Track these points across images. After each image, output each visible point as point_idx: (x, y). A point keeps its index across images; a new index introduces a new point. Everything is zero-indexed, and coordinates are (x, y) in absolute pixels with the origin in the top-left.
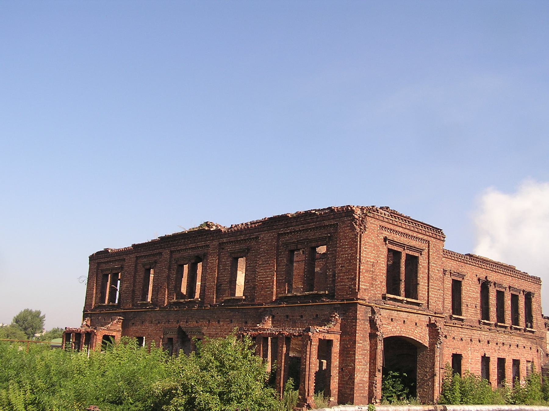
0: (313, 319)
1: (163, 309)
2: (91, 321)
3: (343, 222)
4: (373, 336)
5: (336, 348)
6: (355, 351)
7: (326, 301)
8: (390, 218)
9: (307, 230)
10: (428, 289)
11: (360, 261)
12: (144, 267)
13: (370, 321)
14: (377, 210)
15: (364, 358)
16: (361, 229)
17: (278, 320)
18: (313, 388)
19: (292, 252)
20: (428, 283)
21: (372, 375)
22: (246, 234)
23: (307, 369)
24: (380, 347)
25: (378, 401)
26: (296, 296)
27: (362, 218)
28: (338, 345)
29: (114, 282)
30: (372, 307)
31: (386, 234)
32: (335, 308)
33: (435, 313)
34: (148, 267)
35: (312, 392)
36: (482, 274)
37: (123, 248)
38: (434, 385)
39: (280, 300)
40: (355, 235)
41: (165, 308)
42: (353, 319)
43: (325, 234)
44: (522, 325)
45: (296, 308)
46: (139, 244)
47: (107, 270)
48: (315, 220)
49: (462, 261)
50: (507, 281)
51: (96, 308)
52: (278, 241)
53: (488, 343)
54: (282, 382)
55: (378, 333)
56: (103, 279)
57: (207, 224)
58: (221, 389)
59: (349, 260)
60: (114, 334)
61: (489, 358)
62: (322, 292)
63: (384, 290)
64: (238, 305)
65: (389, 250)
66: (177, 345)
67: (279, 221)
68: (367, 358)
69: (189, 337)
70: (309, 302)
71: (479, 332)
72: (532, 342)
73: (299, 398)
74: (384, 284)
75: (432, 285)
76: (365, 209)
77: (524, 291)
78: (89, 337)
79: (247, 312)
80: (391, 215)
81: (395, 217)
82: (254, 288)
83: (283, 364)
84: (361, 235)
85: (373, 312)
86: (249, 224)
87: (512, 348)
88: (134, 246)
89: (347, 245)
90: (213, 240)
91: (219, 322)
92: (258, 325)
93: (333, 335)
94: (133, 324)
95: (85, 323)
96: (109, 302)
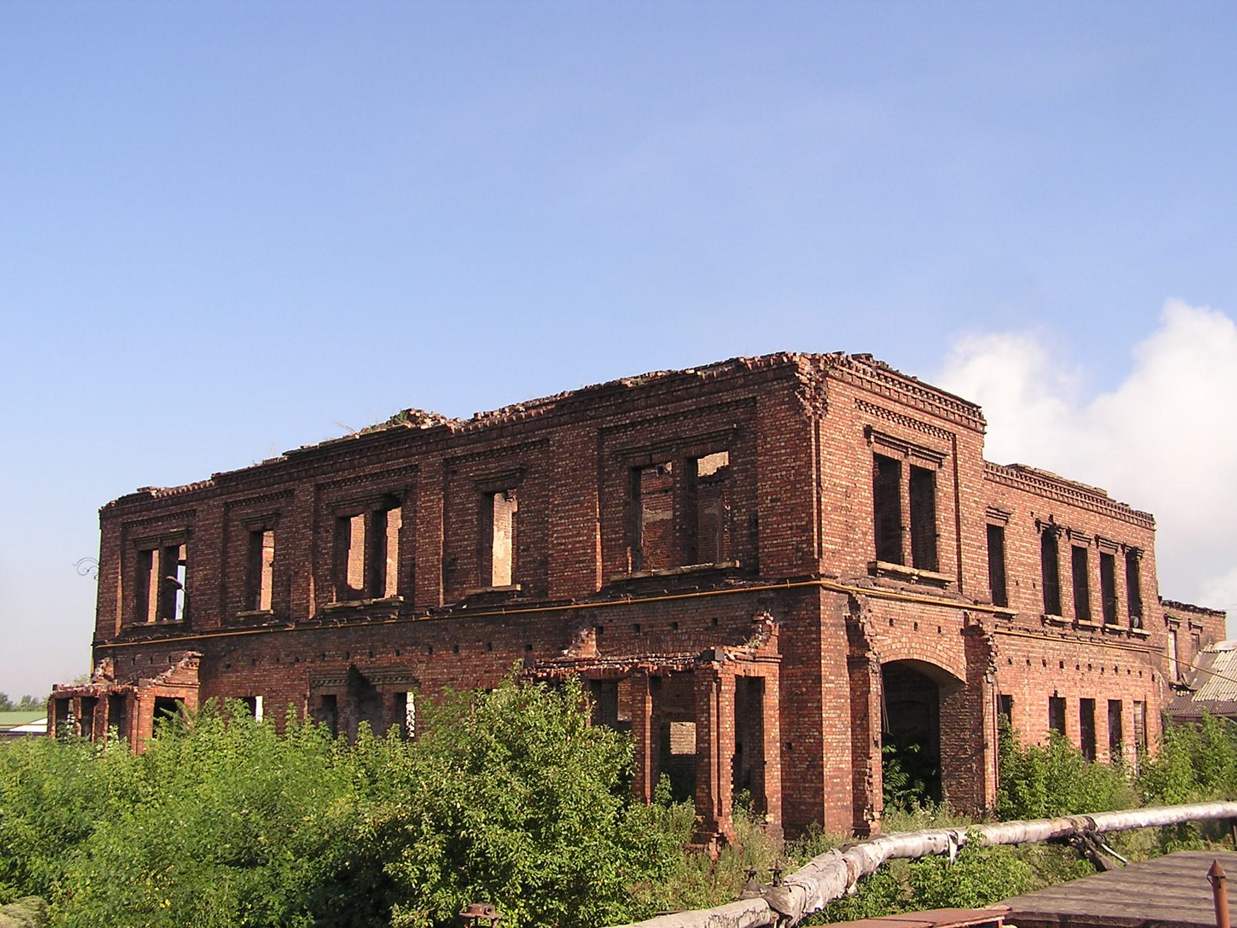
0: (706, 629)
1: (305, 626)
2: (115, 664)
3: (770, 393)
4: (857, 663)
5: (772, 697)
6: (820, 701)
7: (739, 585)
8: (875, 380)
10: (959, 547)
11: (819, 485)
12: (246, 527)
13: (848, 627)
14: (849, 363)
15: (839, 716)
16: (815, 407)
17: (613, 639)
18: (729, 794)
19: (637, 471)
20: (958, 534)
21: (860, 754)
22: (514, 435)
23: (714, 751)
24: (876, 686)
25: (877, 815)
26: (657, 578)
27: (817, 382)
28: (776, 689)
29: (169, 568)
30: (850, 595)
31: (868, 418)
32: (761, 601)
33: (976, 603)
34: (257, 527)
36: (1043, 509)
37: (188, 483)
38: (983, 770)
39: (614, 588)
40: (804, 422)
41: (310, 623)
44: (1123, 625)
45: (660, 605)
46: (232, 473)
47: (149, 539)
48: (696, 391)
49: (1003, 481)
51: (125, 633)
52: (600, 447)
53: (1062, 667)
54: (648, 785)
55: (870, 655)
56: (138, 562)
57: (408, 414)
58: (528, 813)
59: (793, 484)
60: (182, 693)
62: (724, 565)
63: (871, 549)
64: (507, 608)
65: (876, 456)
66: (348, 711)
67: (601, 398)
68: (847, 716)
69: (379, 689)
70: (694, 591)
71: (1043, 642)
72: (1142, 659)
73: (697, 822)
74: (871, 537)
75: (966, 538)
77: (1124, 546)
78: (120, 706)
79: (530, 624)
80: (878, 375)
81: (886, 378)
82: (544, 563)
83: (648, 742)
84: (817, 423)
85: (854, 606)
86: (521, 408)
87: (1106, 675)
88: (218, 477)
89: (783, 448)
90: (427, 452)
91: (456, 649)
92: (566, 652)
93: (764, 666)
94: (229, 666)
95: (100, 672)
96: (159, 618)
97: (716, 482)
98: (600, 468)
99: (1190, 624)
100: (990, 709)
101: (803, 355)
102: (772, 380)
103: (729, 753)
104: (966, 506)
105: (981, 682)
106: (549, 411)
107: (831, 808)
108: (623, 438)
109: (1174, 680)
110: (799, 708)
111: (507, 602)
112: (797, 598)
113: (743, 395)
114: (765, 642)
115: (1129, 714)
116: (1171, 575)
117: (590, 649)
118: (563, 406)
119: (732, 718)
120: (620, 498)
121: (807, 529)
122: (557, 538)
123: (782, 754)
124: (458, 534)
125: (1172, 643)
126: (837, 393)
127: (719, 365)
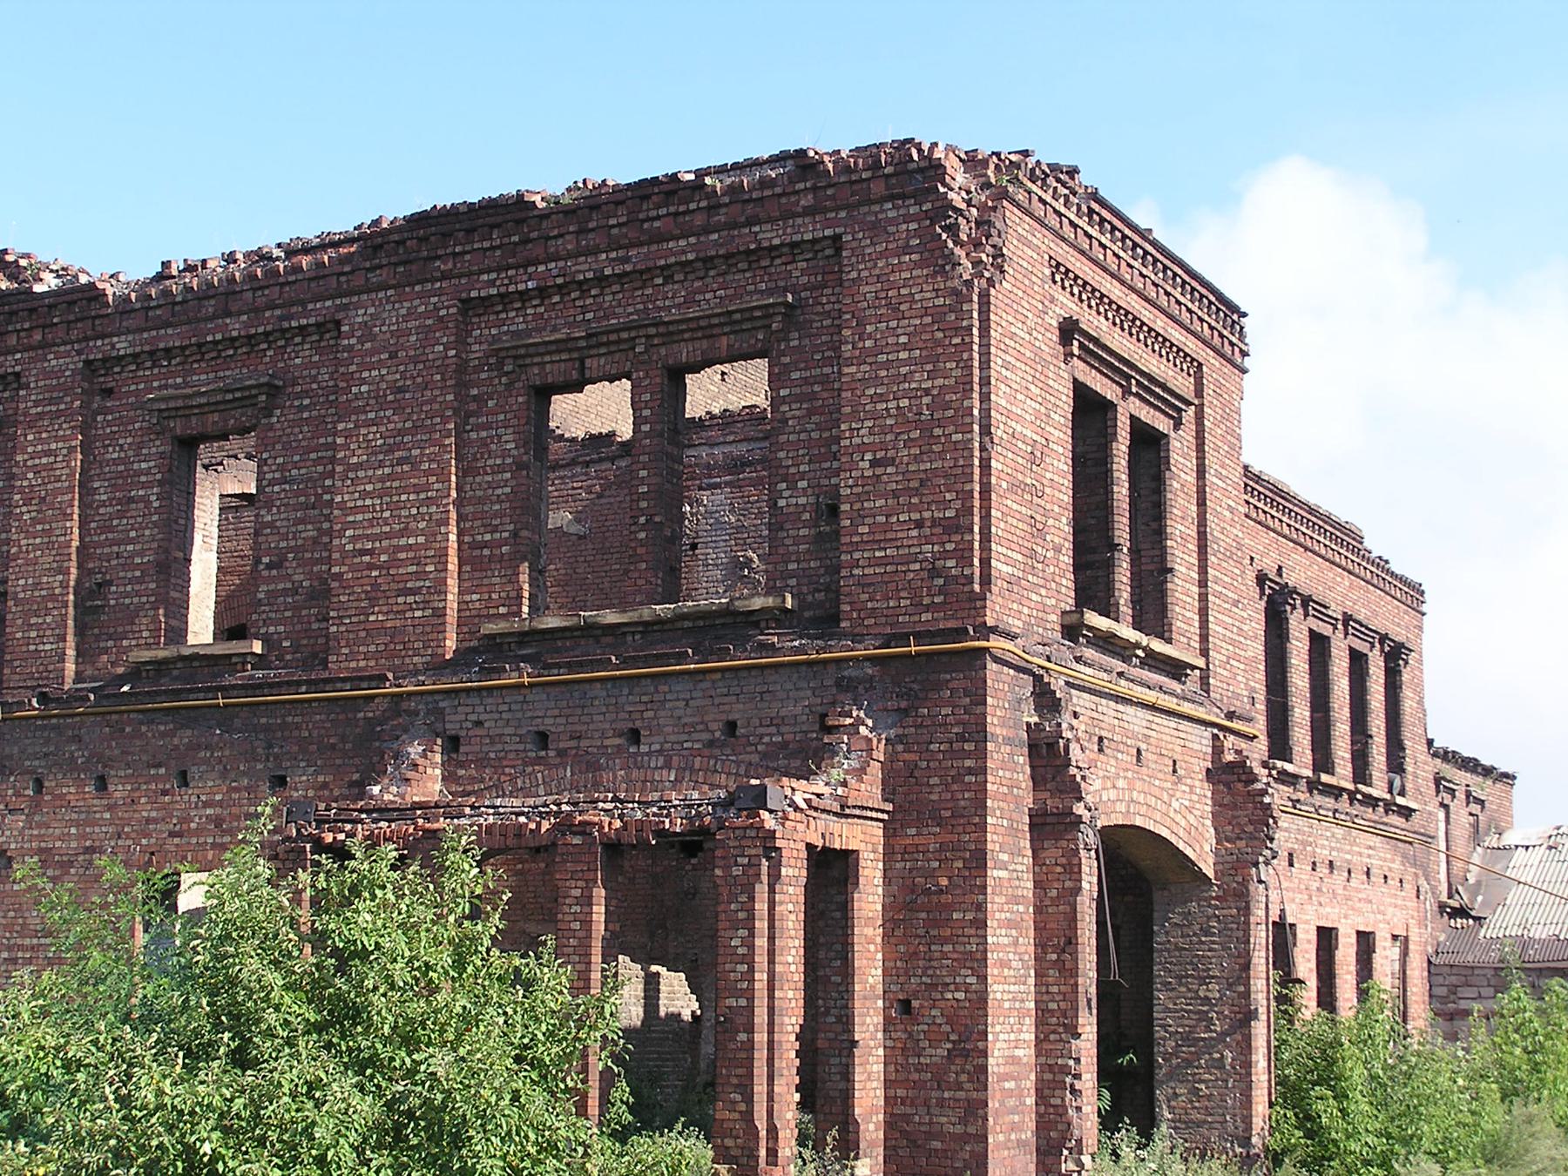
0: (711, 744)
3: (876, 229)
4: (1052, 825)
6: (981, 907)
7: (790, 647)
9: (643, 276)
10: (1203, 598)
11: (986, 430)
15: (1016, 943)
16: (977, 263)
21: (1053, 1026)
22: (256, 310)
26: (591, 631)
27: (982, 208)
28: (879, 881)
30: (1038, 679)
31: (1067, 305)
32: (847, 685)
33: (1231, 716)
35: (788, 1147)
36: (1270, 552)
38: (1248, 1065)
39: (488, 651)
40: (956, 293)
42: (962, 738)
43: (769, 292)
48: (699, 220)
50: (1340, 591)
52: (461, 342)
55: (1079, 809)
61: (1292, 926)
62: (758, 603)
64: (226, 690)
65: (1081, 393)
67: (469, 231)
70: (681, 658)
72: (1404, 856)
74: (1067, 559)
76: (992, 167)
80: (1091, 211)
82: (321, 593)
85: (1046, 700)
86: (277, 253)
87: (1354, 883)
89: (905, 347)
90: (45, 345)
91: (102, 784)
92: (376, 790)
98: (462, 386)
99: (1468, 794)
100: (1260, 938)
101: (950, 149)
103: (791, 1021)
104: (1217, 514)
105: (1245, 883)
106: (343, 260)
107: (998, 1146)
108: (517, 321)
109: (1444, 898)
110: (932, 923)
111: (229, 680)
112: (931, 672)
114: (860, 772)
115: (1385, 958)
116: (1453, 701)
117: (430, 784)
118: (377, 248)
119: (799, 942)
120: (505, 453)
121: (958, 526)
122: (354, 539)
124: (111, 529)
125: (1442, 826)
126: (1020, 238)
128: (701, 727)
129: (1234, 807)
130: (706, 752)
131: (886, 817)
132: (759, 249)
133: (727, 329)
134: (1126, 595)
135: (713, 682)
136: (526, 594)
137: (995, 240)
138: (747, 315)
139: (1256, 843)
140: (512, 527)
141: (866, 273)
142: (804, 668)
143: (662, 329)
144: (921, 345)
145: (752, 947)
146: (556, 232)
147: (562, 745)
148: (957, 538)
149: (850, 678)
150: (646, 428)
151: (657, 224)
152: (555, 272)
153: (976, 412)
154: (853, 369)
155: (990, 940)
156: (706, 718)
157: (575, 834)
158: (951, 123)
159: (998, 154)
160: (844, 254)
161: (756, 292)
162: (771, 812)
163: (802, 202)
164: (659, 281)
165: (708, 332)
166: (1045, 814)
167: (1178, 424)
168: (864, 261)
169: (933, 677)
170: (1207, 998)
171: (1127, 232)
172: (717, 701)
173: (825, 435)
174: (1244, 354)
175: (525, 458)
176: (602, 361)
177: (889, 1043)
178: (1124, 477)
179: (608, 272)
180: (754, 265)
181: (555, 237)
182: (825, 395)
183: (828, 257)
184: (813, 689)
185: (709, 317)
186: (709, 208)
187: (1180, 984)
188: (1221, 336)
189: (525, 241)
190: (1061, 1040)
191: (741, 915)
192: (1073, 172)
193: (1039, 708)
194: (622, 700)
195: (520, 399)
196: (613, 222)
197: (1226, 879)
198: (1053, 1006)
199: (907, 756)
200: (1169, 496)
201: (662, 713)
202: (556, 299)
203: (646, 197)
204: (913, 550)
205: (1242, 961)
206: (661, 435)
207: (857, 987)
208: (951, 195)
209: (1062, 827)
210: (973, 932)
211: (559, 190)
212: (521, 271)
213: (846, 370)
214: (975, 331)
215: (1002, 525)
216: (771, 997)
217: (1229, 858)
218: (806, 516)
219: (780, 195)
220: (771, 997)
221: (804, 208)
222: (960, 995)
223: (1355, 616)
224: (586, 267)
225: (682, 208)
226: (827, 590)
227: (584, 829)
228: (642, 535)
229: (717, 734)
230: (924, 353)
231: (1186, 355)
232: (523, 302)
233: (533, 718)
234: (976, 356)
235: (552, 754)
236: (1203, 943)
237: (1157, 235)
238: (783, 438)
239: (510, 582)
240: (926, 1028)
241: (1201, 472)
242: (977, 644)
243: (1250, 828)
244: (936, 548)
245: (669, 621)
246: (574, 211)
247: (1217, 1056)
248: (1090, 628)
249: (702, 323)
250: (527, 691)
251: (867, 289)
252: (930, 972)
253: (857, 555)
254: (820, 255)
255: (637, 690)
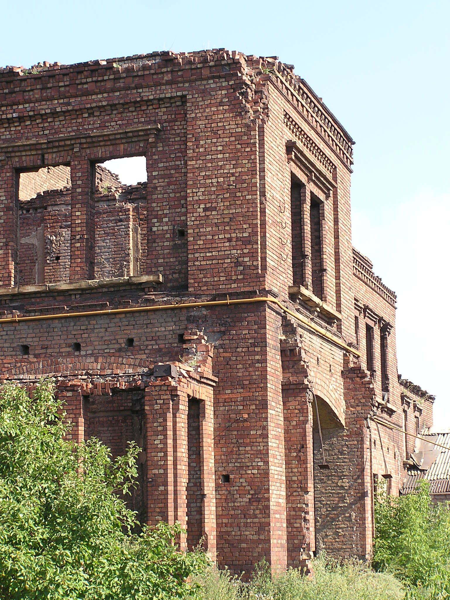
0: (120, 350)
3: (205, 93)
6: (265, 428)
7: (162, 301)
9: (78, 112)
11: (263, 194)
13: (283, 352)
21: (295, 488)
38: (364, 519)
40: (247, 126)
42: (254, 345)
48: (109, 85)
55: (306, 382)
58: (42, 533)
89: (221, 152)
97: (36, 209)
99: (415, 406)
101: (241, 54)
102: (209, 78)
103: (183, 481)
105: (361, 428)
110: (242, 437)
113: (168, 92)
114: (204, 361)
119: (186, 442)
121: (249, 241)
123: (218, 487)
127: (140, 58)
128: (114, 342)
129: (355, 390)
130: (117, 354)
131: (214, 384)
132: (142, 101)
133: (124, 141)
134: (310, 281)
135: (120, 319)
136: (13, 275)
137: (264, 100)
138: (136, 134)
139: (367, 408)
140: (4, 240)
141: (200, 115)
142: (169, 312)
143: (89, 140)
144: (229, 151)
145: (166, 444)
146: (29, 88)
147: (37, 352)
148: (249, 247)
149: (194, 316)
150: (79, 190)
151: (85, 86)
152: (28, 109)
153: (258, 185)
154: (193, 162)
155: (270, 444)
156: (117, 337)
157: (68, 391)
158: (243, 42)
159: (263, 58)
160: (188, 105)
161: (139, 123)
162: (172, 378)
163: (165, 78)
164: (86, 115)
165: (114, 142)
166: (290, 384)
167: (328, 197)
168: (198, 109)
169: (239, 315)
170: (342, 486)
171: (313, 99)
172: (122, 328)
173: (178, 195)
174: (351, 163)
175: (11, 205)
176: (54, 155)
177: (218, 497)
178: (309, 222)
179: (58, 110)
180: (138, 109)
181: (29, 91)
182: (177, 175)
183: (178, 106)
184: (175, 322)
185: (115, 134)
186: (114, 79)
187: (328, 480)
188: (344, 154)
189: (11, 93)
190: (299, 495)
191: (160, 428)
192: (291, 68)
193: (285, 332)
194: (71, 328)
195: (8, 174)
196: (61, 84)
197: (351, 426)
198: (295, 478)
199: (225, 355)
200: (324, 233)
201: (93, 335)
202: (28, 123)
203: (81, 72)
204: (226, 253)
205: (360, 467)
206: (87, 194)
207: (205, 468)
208: (244, 78)
209: (298, 391)
210: (261, 440)
211: (28, 67)
212: (9, 108)
213: (189, 163)
214: (257, 145)
215: (270, 241)
216: (175, 468)
217: (353, 416)
218: (168, 236)
219: (153, 74)
220: (175, 468)
221: (166, 81)
222: (255, 472)
223: (371, 307)
224: (46, 107)
225: (100, 79)
226: (180, 273)
227: (73, 388)
228: (78, 245)
229: (123, 345)
230: (231, 155)
231: (331, 162)
232: (9, 124)
233: (20, 338)
234: (258, 157)
235: (31, 356)
236: (339, 458)
237: (324, 101)
238: (155, 197)
239: (4, 269)
240: (237, 488)
241: (336, 221)
242: (261, 299)
243: (363, 401)
244: (239, 252)
245: (96, 288)
246: (40, 78)
247: (347, 515)
248: (302, 295)
249: (111, 137)
250: (17, 324)
251: (200, 123)
252: (239, 461)
253: (197, 255)
254: (173, 105)
255: (78, 323)
